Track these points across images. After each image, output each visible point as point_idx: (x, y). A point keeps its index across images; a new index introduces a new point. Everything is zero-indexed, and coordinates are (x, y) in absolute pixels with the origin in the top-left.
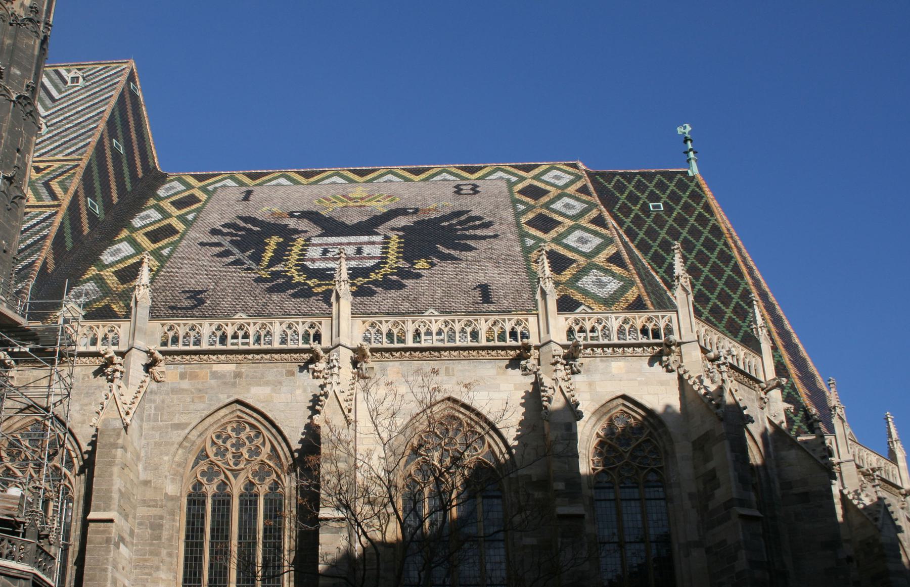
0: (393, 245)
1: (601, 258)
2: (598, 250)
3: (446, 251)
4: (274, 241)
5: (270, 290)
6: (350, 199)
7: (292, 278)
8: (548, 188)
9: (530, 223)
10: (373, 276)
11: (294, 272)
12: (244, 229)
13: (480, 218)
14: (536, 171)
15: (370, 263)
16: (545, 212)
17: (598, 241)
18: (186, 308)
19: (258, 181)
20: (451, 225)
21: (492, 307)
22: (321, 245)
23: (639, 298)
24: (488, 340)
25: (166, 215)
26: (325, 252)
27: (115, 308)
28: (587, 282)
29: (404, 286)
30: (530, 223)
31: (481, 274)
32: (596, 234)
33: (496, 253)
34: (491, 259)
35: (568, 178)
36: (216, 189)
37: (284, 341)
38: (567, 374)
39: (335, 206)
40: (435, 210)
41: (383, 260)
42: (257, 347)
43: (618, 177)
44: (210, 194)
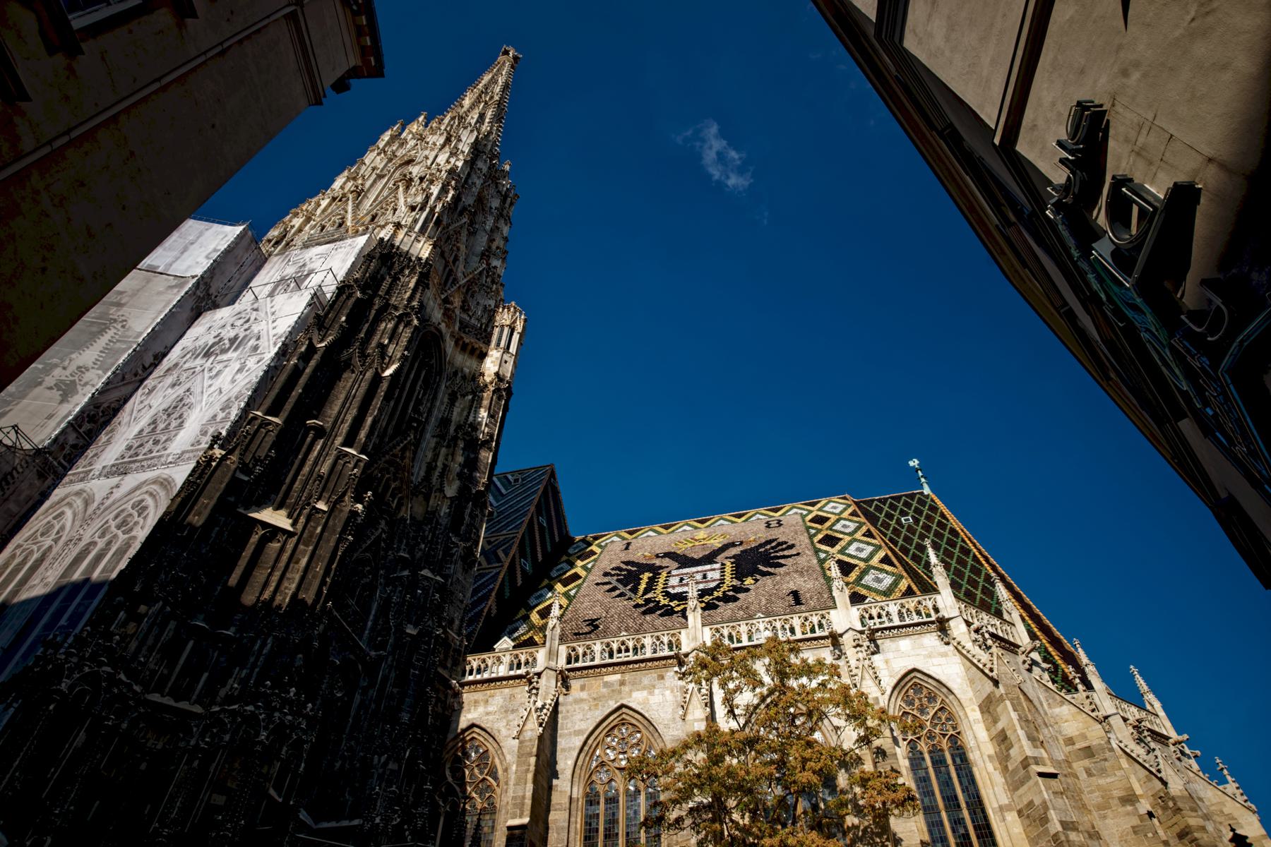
0: (728, 569)
1: (875, 561)
2: (871, 555)
3: (765, 569)
4: (646, 576)
5: (644, 613)
6: (696, 540)
7: (659, 602)
8: (829, 515)
9: (820, 542)
10: (716, 594)
11: (660, 598)
12: (626, 570)
13: (786, 543)
14: (819, 506)
15: (712, 585)
16: (830, 532)
17: (870, 549)
18: (586, 633)
19: (634, 536)
20: (766, 550)
21: (803, 608)
22: (678, 575)
24: (803, 633)
26: (682, 579)
27: (536, 638)
28: (868, 579)
29: (738, 599)
30: (820, 542)
31: (792, 583)
32: (868, 544)
33: (801, 566)
34: (797, 571)
35: (841, 507)
36: (607, 544)
37: (655, 652)
38: (867, 655)
39: (686, 546)
40: (754, 540)
41: (722, 581)
42: (636, 658)
43: (875, 502)
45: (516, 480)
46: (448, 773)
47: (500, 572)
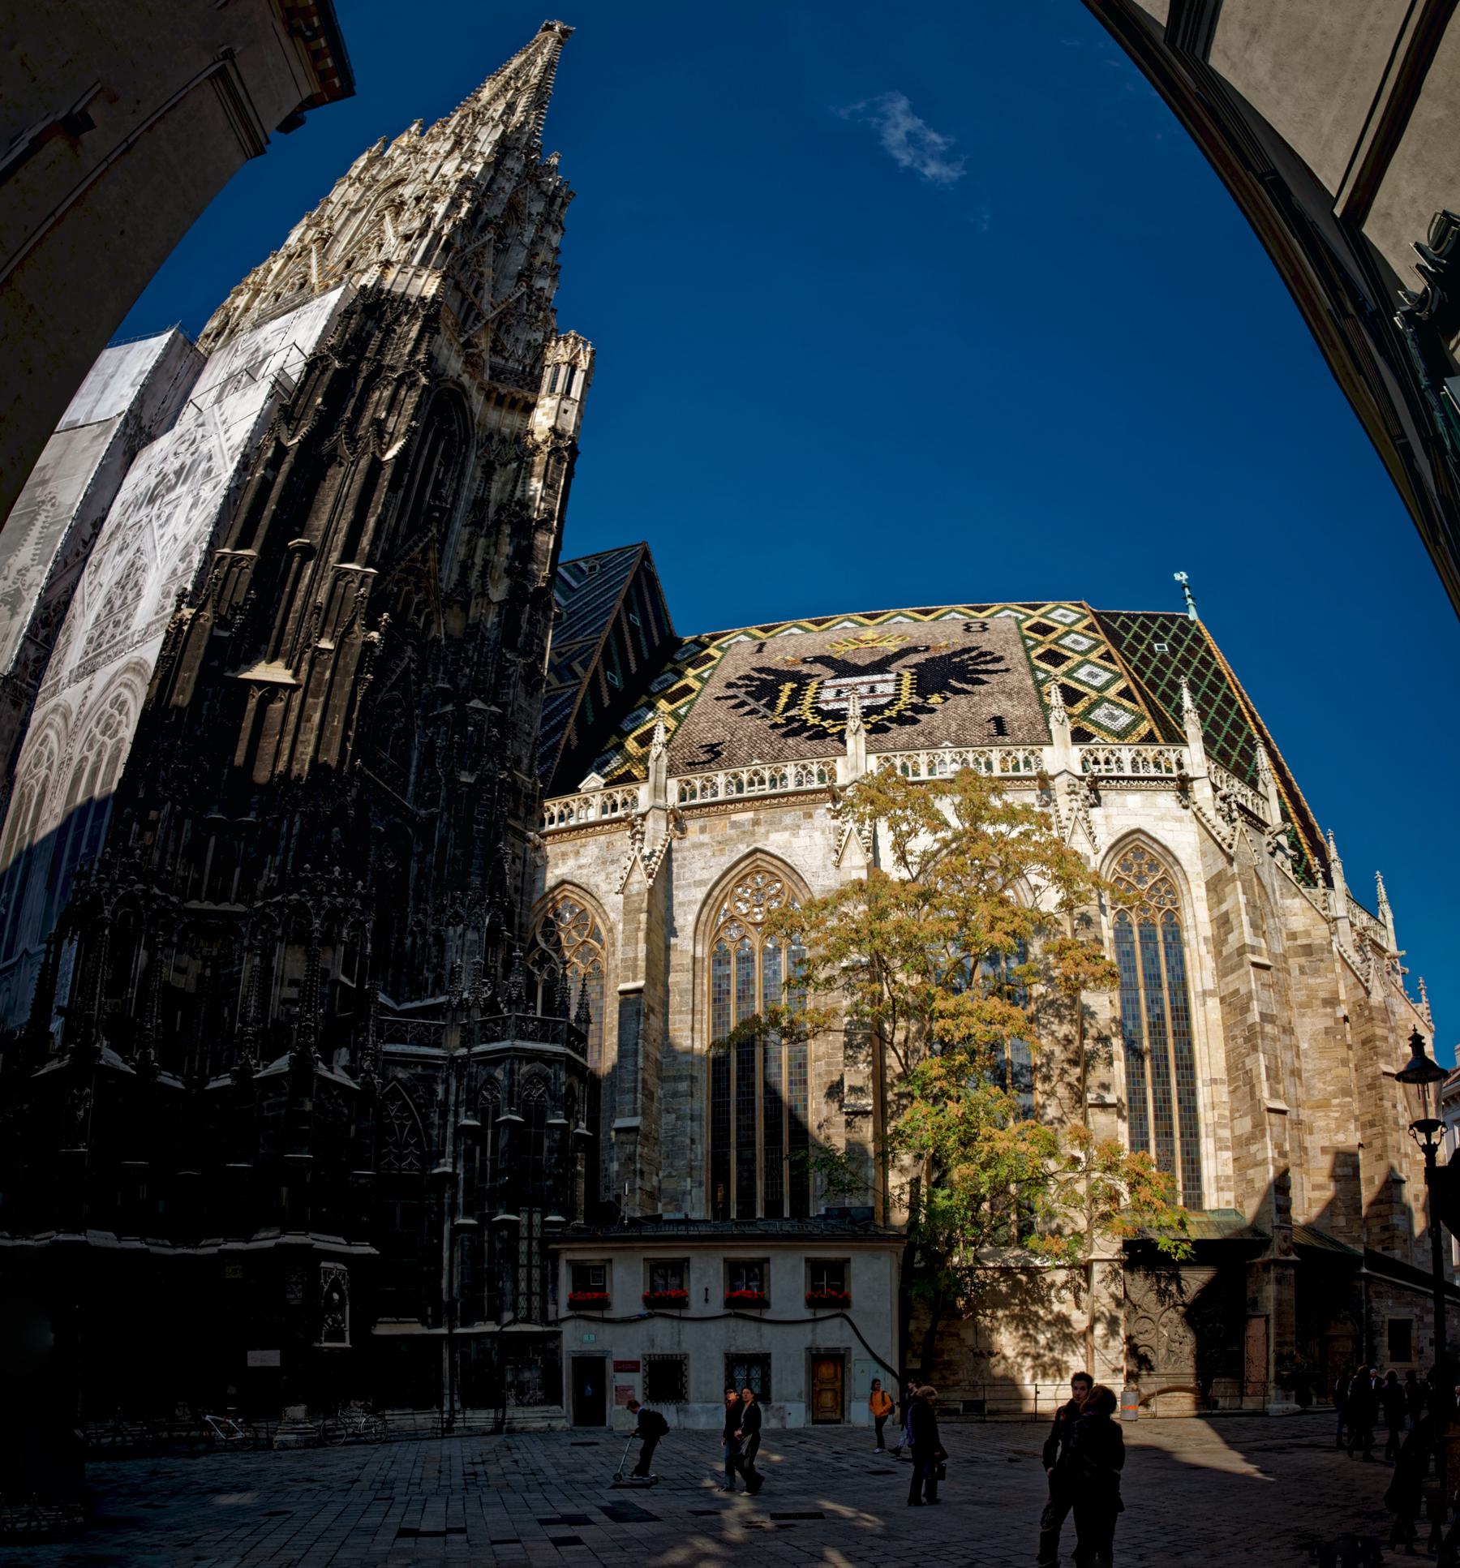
23: (1151, 732)
45: (592, 568)
46: (539, 938)
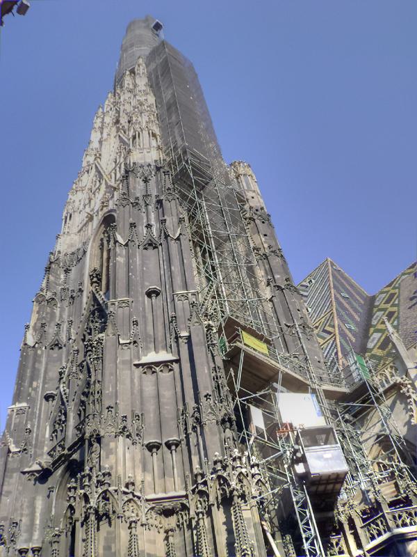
25: (384, 310)
44: (398, 288)
47: (335, 339)
